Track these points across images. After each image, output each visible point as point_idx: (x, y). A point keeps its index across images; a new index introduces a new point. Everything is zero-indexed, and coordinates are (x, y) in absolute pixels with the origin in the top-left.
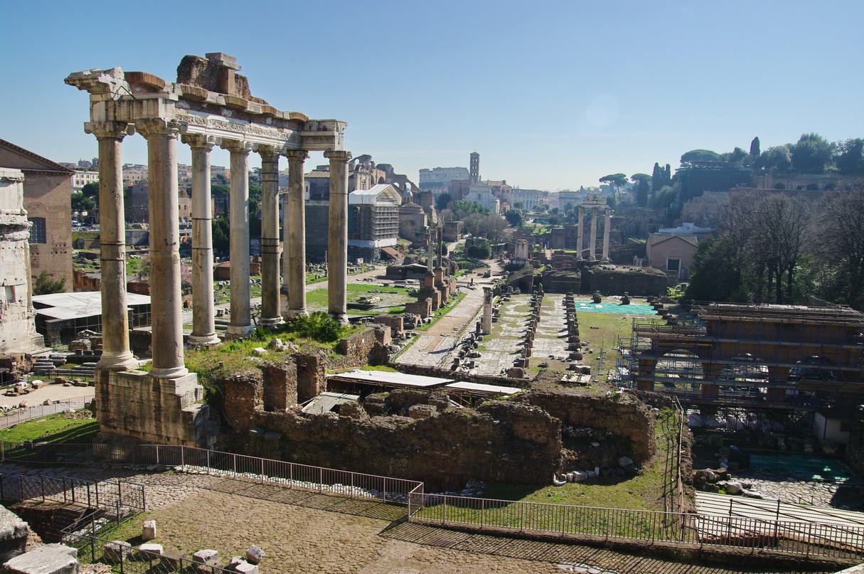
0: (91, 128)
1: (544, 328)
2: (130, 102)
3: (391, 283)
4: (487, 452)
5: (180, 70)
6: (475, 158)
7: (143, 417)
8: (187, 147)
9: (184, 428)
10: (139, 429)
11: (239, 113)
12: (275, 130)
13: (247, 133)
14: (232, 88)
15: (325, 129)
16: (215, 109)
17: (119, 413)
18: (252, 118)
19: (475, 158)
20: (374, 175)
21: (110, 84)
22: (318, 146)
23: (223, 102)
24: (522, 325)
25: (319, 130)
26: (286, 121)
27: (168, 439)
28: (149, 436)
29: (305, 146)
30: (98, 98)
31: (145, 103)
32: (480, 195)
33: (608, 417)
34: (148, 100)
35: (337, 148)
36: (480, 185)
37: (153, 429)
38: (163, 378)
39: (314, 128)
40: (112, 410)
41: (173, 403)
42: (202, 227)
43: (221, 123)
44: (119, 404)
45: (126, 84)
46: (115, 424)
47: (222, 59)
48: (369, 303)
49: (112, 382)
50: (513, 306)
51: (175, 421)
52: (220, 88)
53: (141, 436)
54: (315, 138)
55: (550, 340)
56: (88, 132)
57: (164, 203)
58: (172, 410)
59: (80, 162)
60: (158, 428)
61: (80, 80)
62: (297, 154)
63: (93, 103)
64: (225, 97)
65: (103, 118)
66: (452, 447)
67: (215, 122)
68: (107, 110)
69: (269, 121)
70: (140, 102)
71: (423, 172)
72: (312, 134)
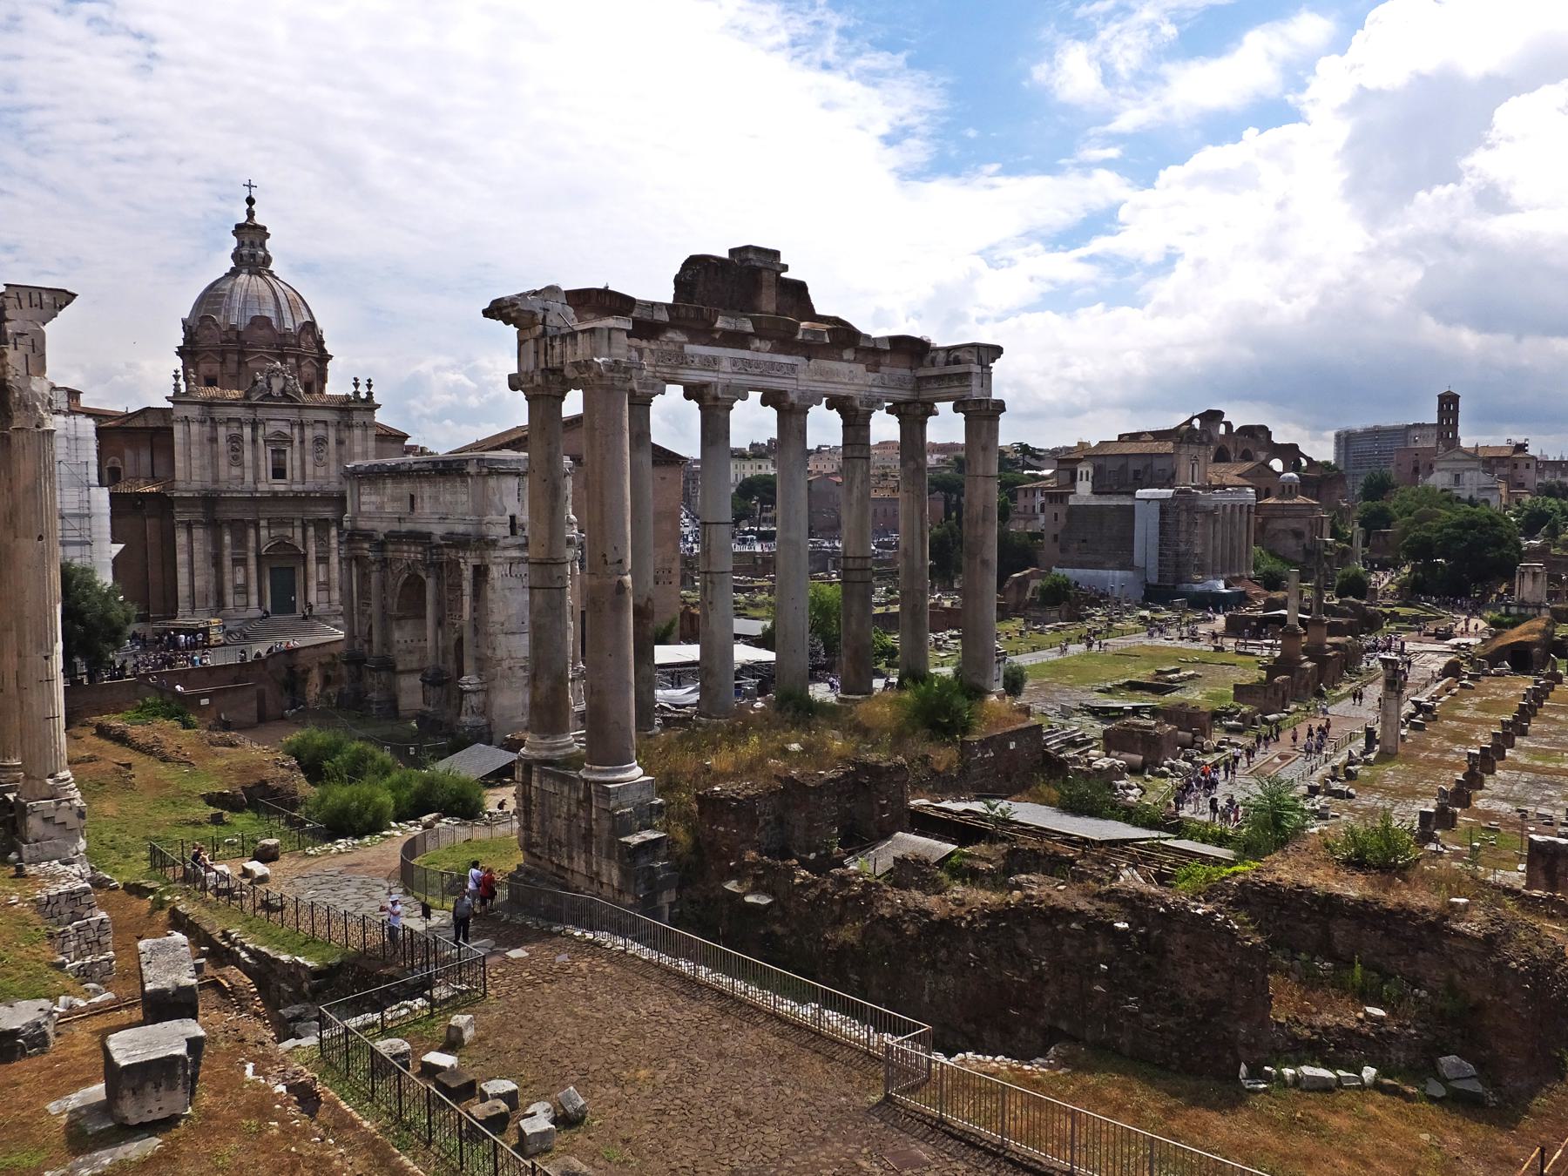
0: (516, 382)
1: (1528, 750)
2: (563, 337)
3: (1230, 643)
4: (1098, 988)
5: (678, 281)
6: (1449, 403)
7: (570, 844)
8: (694, 404)
9: (620, 869)
10: (565, 863)
11: (786, 342)
12: (862, 367)
13: (802, 376)
14: (768, 302)
15: (957, 361)
16: (736, 339)
17: (543, 833)
18: (810, 350)
19: (1449, 403)
20: (1231, 448)
21: (538, 310)
22: (944, 392)
23: (748, 327)
24: (1483, 738)
25: (948, 363)
26: (885, 352)
27: (602, 884)
28: (578, 877)
29: (925, 396)
30: (527, 335)
31: (580, 336)
32: (1457, 477)
33: (1421, 955)
34: (583, 332)
35: (976, 392)
36: (1459, 456)
37: (583, 870)
38: (598, 783)
39: (942, 356)
40: (535, 827)
41: (606, 824)
42: (713, 536)
43: (748, 363)
44: (543, 823)
45: (570, 310)
46: (537, 851)
47: (751, 256)
48: (1170, 681)
49: (535, 783)
50: (1477, 700)
51: (609, 857)
52: (744, 303)
53: (568, 876)
54: (939, 378)
55: (1531, 776)
56: (513, 387)
57: (602, 494)
58: (605, 836)
59: (753, 446)
60: (588, 864)
61: (499, 309)
62: (913, 416)
63: (521, 343)
64: (752, 319)
65: (532, 367)
66: (1031, 965)
67: (734, 361)
68: (537, 352)
69: (848, 354)
70: (573, 335)
71: (1345, 441)
72: (934, 372)
